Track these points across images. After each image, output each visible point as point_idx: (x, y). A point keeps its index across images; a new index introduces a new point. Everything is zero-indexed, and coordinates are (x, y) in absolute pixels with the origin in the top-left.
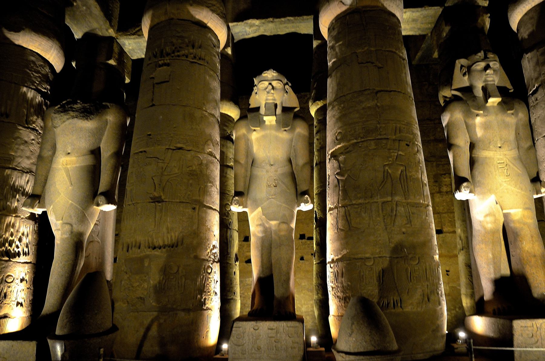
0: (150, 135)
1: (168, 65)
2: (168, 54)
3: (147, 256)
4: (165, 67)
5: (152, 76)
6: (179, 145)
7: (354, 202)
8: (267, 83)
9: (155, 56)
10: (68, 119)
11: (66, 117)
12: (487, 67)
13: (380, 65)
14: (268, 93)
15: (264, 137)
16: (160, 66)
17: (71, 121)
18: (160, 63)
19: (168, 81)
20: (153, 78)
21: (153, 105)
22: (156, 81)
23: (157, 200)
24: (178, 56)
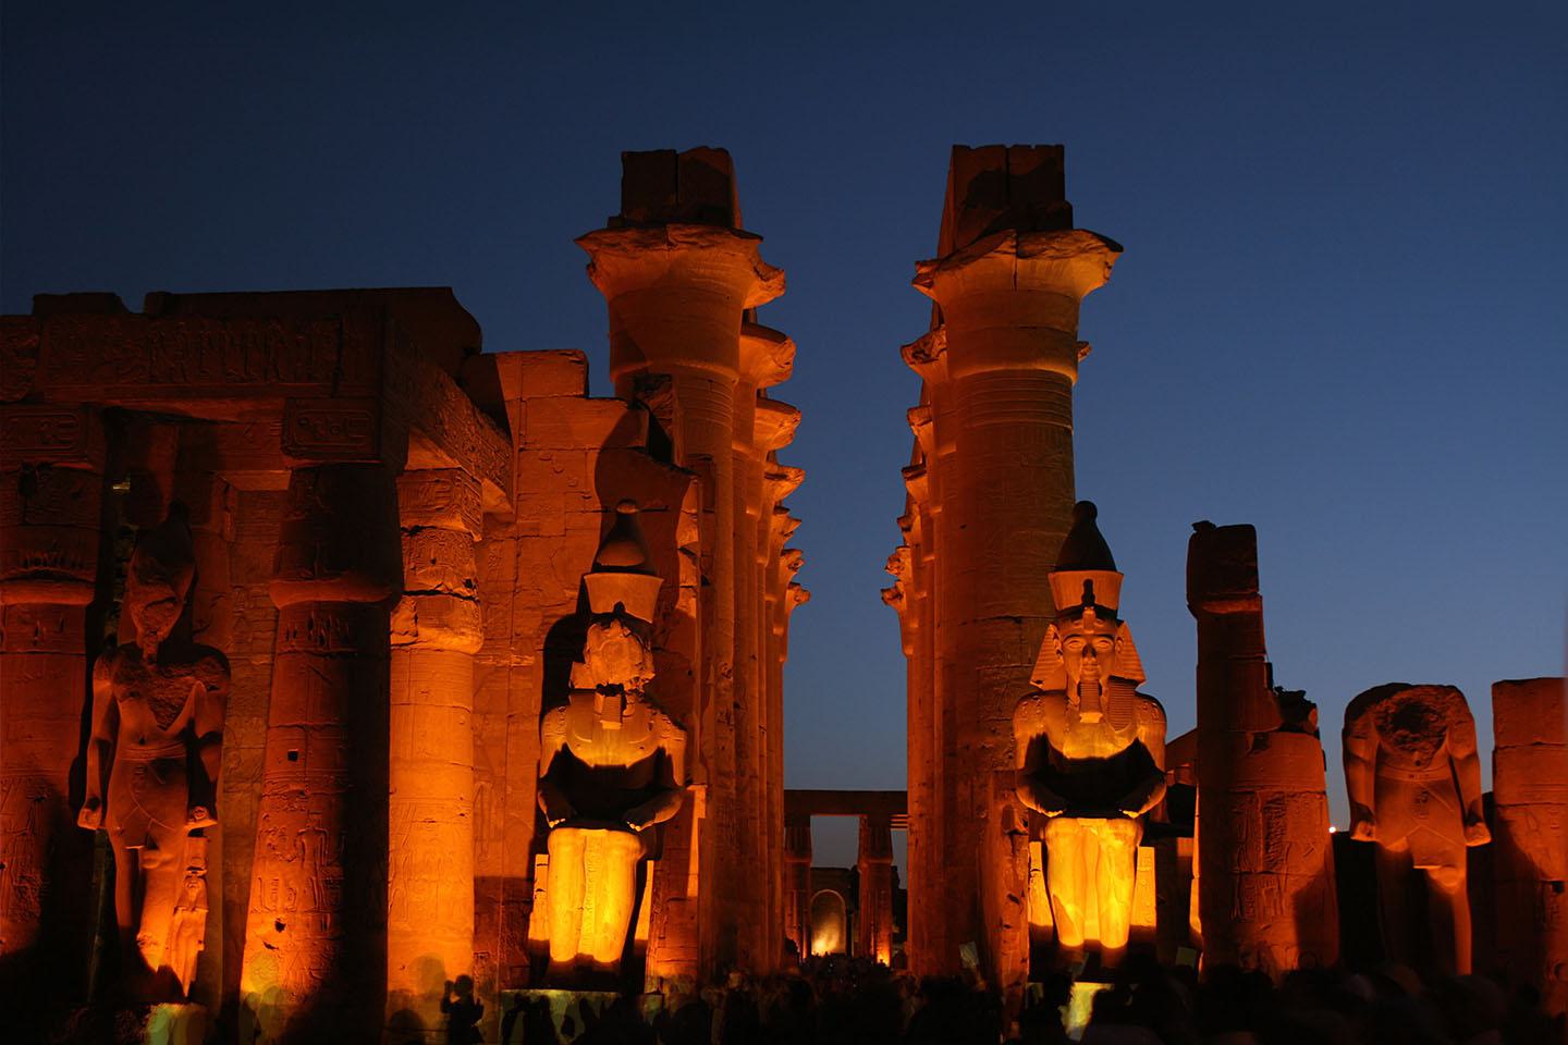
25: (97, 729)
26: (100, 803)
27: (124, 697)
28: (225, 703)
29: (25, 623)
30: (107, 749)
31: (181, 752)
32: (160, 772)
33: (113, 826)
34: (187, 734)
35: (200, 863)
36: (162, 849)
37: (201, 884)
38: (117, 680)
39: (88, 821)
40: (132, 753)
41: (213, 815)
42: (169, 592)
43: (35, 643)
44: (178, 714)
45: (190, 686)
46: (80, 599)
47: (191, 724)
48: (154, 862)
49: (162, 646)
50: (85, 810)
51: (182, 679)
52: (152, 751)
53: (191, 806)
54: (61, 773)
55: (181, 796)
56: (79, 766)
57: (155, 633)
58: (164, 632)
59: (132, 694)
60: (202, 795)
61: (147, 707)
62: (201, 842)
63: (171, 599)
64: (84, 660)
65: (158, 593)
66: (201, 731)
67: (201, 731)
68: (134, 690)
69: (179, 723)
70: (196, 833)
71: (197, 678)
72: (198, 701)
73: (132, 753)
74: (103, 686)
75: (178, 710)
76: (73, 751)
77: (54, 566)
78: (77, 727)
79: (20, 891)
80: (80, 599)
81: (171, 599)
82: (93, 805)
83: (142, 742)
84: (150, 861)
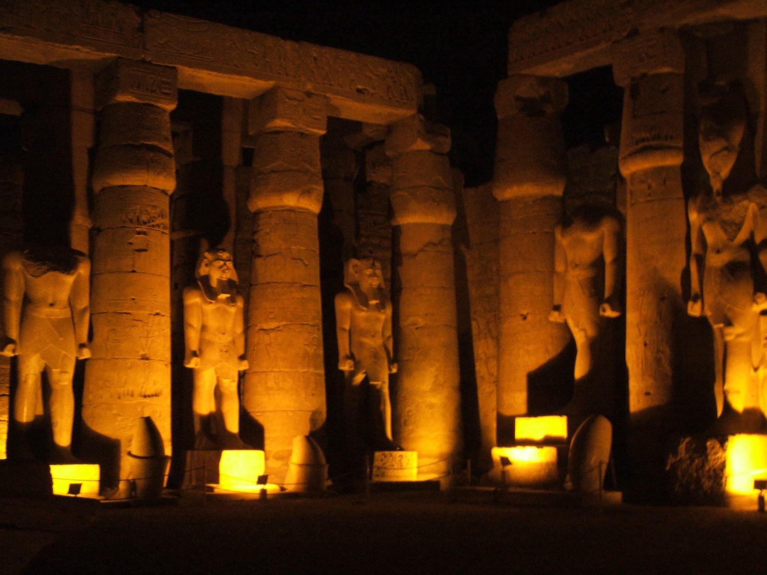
0: (133, 299)
1: (145, 233)
2: (145, 223)
3: (140, 403)
5: (129, 241)
6: (158, 311)
7: (282, 370)
8: (222, 263)
9: (131, 221)
10: (48, 270)
11: (45, 267)
12: (374, 275)
13: (307, 263)
14: (224, 271)
15: (218, 309)
16: (139, 233)
19: (145, 250)
20: (131, 243)
21: (134, 271)
22: (133, 247)
24: (153, 226)
25: (695, 248)
27: (704, 222)
29: (642, 182)
30: (701, 261)
31: (745, 256)
33: (708, 313)
39: (694, 310)
40: (716, 261)
42: (723, 143)
43: (649, 195)
44: (740, 229)
45: (746, 209)
46: (674, 160)
47: (752, 234)
48: (732, 334)
49: (726, 183)
50: (690, 303)
51: (740, 204)
53: (755, 293)
54: (675, 278)
55: (747, 286)
56: (686, 273)
57: (718, 174)
58: (725, 173)
63: (726, 148)
64: (683, 201)
65: (716, 145)
66: (758, 239)
69: (742, 236)
71: (750, 201)
72: (755, 216)
74: (694, 217)
75: (739, 226)
76: (682, 265)
78: (682, 247)
79: (658, 361)
80: (674, 160)
81: (726, 148)
82: (695, 300)
83: (718, 252)
84: (730, 334)
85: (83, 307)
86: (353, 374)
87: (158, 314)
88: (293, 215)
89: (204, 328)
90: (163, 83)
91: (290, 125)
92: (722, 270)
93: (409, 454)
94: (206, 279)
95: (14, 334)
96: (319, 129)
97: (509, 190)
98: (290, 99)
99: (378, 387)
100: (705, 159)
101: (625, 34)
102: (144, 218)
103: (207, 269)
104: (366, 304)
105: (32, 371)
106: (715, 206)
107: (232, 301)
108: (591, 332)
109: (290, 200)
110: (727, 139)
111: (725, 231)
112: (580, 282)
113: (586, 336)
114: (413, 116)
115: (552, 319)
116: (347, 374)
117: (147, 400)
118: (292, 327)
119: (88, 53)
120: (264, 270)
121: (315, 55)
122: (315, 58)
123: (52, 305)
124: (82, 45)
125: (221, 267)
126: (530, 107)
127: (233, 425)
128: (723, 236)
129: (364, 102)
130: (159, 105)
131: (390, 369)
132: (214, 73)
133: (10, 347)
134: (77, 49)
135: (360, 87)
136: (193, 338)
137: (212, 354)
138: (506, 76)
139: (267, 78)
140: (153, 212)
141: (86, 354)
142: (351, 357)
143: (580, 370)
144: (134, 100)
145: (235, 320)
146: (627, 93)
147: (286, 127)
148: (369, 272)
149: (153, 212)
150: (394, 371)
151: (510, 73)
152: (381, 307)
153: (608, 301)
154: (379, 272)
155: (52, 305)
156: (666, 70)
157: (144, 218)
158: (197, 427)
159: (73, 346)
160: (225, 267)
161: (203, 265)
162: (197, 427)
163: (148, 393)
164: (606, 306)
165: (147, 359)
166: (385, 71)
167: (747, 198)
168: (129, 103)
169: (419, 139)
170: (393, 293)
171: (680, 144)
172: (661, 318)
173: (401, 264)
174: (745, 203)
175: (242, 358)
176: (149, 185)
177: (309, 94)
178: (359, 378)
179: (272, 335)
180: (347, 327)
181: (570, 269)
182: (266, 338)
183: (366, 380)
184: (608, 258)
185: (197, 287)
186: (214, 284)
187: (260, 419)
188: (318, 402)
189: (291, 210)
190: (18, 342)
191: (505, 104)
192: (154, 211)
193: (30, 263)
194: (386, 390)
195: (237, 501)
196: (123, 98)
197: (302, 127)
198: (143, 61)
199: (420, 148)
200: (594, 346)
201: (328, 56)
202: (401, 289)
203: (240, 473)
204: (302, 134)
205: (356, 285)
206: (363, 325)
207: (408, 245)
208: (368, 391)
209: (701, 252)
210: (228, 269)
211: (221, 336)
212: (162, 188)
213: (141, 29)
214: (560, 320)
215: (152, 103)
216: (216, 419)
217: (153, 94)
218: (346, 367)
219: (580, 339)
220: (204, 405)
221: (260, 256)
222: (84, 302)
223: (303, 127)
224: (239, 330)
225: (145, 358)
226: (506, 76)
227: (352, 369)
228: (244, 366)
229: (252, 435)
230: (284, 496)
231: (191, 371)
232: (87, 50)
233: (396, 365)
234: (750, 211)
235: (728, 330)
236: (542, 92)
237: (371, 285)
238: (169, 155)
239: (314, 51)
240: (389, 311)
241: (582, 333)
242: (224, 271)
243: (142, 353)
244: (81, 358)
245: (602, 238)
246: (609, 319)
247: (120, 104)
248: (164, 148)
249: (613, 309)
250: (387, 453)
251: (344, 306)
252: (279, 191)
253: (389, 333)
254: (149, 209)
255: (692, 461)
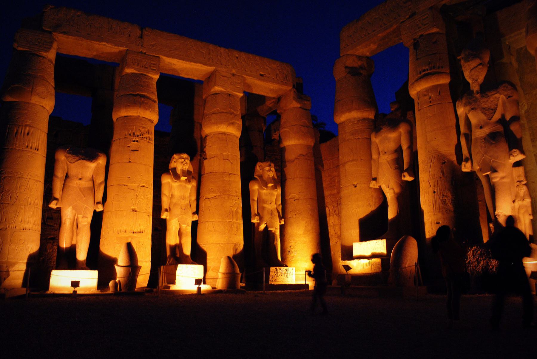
1: (138, 142)
2: (138, 136)
3: (130, 237)
4: (136, 143)
6: (143, 185)
8: (183, 160)
9: (130, 135)
10: (79, 159)
12: (271, 170)
14: (184, 165)
15: (180, 185)
16: (134, 141)
17: (80, 161)
18: (134, 139)
21: (130, 162)
22: (131, 149)
23: (134, 210)
25: (463, 129)
26: (470, 159)
27: (469, 111)
28: (518, 103)
29: (425, 95)
30: (468, 137)
31: (500, 128)
32: (492, 138)
33: (477, 168)
34: (502, 121)
35: (523, 178)
36: (500, 171)
37: (525, 188)
38: (465, 105)
39: (466, 168)
40: (479, 134)
41: (522, 152)
42: (478, 61)
43: (430, 102)
44: (495, 112)
45: (498, 99)
46: (445, 80)
47: (503, 116)
48: (496, 178)
49: (482, 86)
50: (463, 163)
51: (493, 96)
52: (486, 130)
53: (510, 149)
54: (450, 151)
55: (504, 146)
56: (458, 148)
57: (477, 81)
58: (481, 79)
59: (472, 109)
60: (515, 144)
61: (480, 112)
62: (521, 170)
63: (480, 64)
64: (452, 104)
65: (474, 63)
66: (508, 118)
67: (508, 118)
68: (473, 107)
69: (497, 116)
70: (517, 164)
71: (501, 94)
72: (504, 104)
73: (479, 134)
74: (461, 111)
75: (494, 111)
76: (454, 141)
77: (431, 69)
78: (454, 131)
79: (444, 202)
80: (445, 80)
81: (480, 64)
82: (467, 160)
83: (481, 128)
84: (495, 178)
85: (100, 181)
86: (259, 224)
87: (143, 186)
88: (224, 136)
89: (172, 196)
90: (152, 64)
91: (223, 90)
92: (485, 139)
93: (290, 268)
94: (174, 169)
95: (57, 195)
96: (239, 92)
97: (343, 116)
98: (223, 76)
99: (273, 232)
100: (467, 74)
101: (407, 17)
102: (138, 133)
103: (175, 164)
104: (266, 186)
105: (69, 217)
106: (476, 100)
107: (188, 181)
108: (397, 190)
109: (223, 128)
110: (480, 58)
111: (485, 114)
112: (388, 162)
113: (394, 193)
114: (290, 90)
115: (371, 186)
116: (256, 225)
117: (135, 235)
118: (223, 196)
119: (111, 47)
120: (209, 166)
121: (237, 56)
122: (237, 58)
123: (80, 179)
124: (107, 42)
125: (182, 162)
126: (353, 72)
127: (187, 251)
128: (483, 117)
129: (264, 80)
130: (149, 75)
131: (280, 222)
132: (180, 61)
133: (54, 202)
134: (104, 45)
135: (262, 73)
136: (165, 202)
137: (177, 211)
138: (339, 57)
139: (210, 66)
140: (142, 130)
141: (100, 208)
142: (258, 215)
143: (391, 214)
144: (135, 71)
145: (191, 193)
146: (412, 47)
147: (221, 91)
148: (267, 168)
149: (142, 130)
150: (283, 223)
151: (341, 55)
152: (274, 187)
153: (406, 171)
154: (273, 169)
155: (80, 179)
156: (435, 30)
157: (138, 133)
158: (168, 253)
159: (91, 202)
160: (185, 162)
161: (173, 162)
162: (168, 253)
163: (136, 230)
164: (406, 174)
165: (136, 211)
166: (275, 66)
167: (498, 92)
168: (133, 74)
169: (294, 101)
170: (281, 181)
171: (448, 71)
172: (443, 175)
173: (285, 166)
174: (497, 95)
175: (194, 214)
176: (141, 116)
177: (233, 75)
178: (262, 227)
179: (212, 201)
180: (256, 199)
181: (381, 155)
182: (208, 202)
183: (266, 228)
184: (405, 147)
185: (169, 174)
186: (179, 171)
187: (205, 248)
188: (240, 240)
189: (224, 133)
190: (60, 199)
191: (339, 72)
192: (143, 130)
193: (70, 155)
194: (278, 233)
195: (186, 295)
196: (128, 71)
197: (230, 91)
198: (141, 53)
199: (295, 106)
200: (399, 198)
201: (244, 56)
202: (286, 179)
203: (187, 278)
204: (229, 95)
205: (261, 177)
206: (264, 197)
207: (289, 156)
208: (268, 234)
209: (467, 132)
210: (186, 163)
211: (182, 200)
212: (149, 118)
213: (141, 37)
214: (377, 187)
215: (145, 73)
216: (178, 247)
217: (146, 69)
218: (255, 220)
219: (390, 195)
220: (172, 240)
221: (206, 159)
222: (101, 179)
223: (230, 91)
224: (194, 198)
225: (134, 210)
226: (339, 57)
227: (259, 221)
228: (195, 218)
229: (198, 256)
230: (214, 292)
231: (165, 220)
232: (110, 45)
233: (283, 219)
234: (500, 102)
235: (495, 175)
236: (360, 63)
237: (269, 175)
238: (154, 101)
239: (236, 54)
240: (279, 191)
241: (392, 191)
242: (184, 165)
243: (133, 207)
244: (98, 210)
245: (400, 136)
246: (407, 181)
247: (127, 74)
248: (151, 97)
249: (410, 176)
250: (278, 268)
251: (255, 187)
252: (217, 123)
253: (279, 202)
254: (141, 129)
255: (479, 262)
